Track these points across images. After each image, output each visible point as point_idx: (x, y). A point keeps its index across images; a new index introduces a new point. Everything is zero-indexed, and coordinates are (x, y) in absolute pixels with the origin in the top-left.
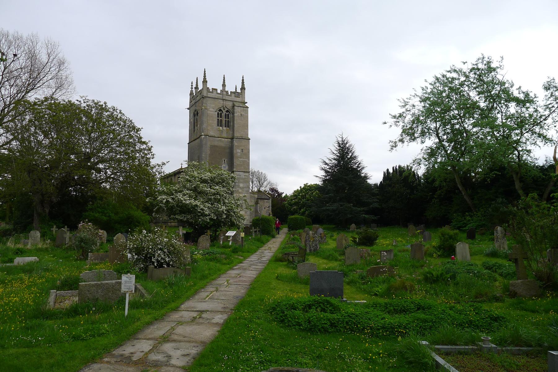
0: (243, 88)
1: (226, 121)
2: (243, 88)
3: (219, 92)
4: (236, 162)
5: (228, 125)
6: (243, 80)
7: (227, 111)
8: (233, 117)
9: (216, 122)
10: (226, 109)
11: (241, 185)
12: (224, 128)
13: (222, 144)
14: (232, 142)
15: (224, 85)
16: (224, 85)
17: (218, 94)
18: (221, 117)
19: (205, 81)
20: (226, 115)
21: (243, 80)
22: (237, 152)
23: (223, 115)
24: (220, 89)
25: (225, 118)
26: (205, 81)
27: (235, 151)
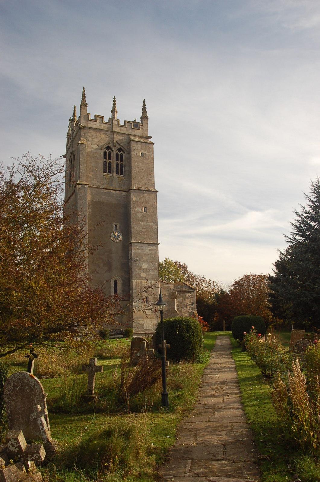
0: (144, 117)
1: (117, 165)
2: (144, 117)
3: (106, 120)
4: (135, 227)
7: (120, 150)
8: (130, 158)
9: (101, 165)
10: (118, 147)
11: (145, 266)
12: (115, 175)
14: (128, 197)
15: (113, 111)
16: (113, 111)
17: (105, 123)
18: (110, 158)
19: (84, 105)
20: (117, 156)
21: (144, 105)
22: (137, 211)
23: (114, 155)
24: (107, 116)
25: (117, 160)
26: (84, 105)
27: (132, 211)
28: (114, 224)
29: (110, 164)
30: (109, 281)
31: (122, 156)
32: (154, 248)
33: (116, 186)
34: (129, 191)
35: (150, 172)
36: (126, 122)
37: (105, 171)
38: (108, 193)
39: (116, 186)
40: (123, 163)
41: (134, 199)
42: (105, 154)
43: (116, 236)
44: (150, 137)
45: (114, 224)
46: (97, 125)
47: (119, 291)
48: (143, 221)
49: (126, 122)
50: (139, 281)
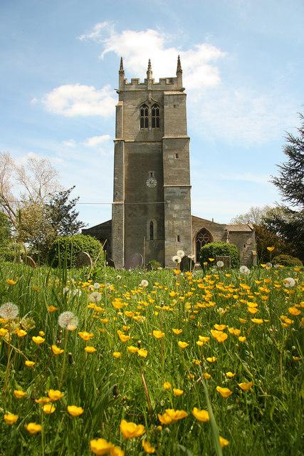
0: (179, 72)
1: (153, 119)
2: (179, 72)
3: (142, 81)
4: (167, 173)
5: (158, 126)
6: (179, 61)
8: (163, 112)
11: (177, 207)
13: (145, 151)
18: (147, 114)
20: (153, 111)
21: (179, 61)
22: (169, 157)
23: (150, 111)
27: (164, 158)
28: (150, 172)
29: (147, 120)
30: (146, 221)
31: (158, 111)
32: (186, 190)
33: (151, 138)
34: (161, 141)
35: (182, 121)
36: (160, 80)
37: (142, 126)
38: (144, 145)
39: (151, 138)
40: (159, 117)
41: (166, 147)
42: (142, 111)
43: (151, 183)
44: (184, 89)
45: (150, 172)
46: (133, 88)
47: (155, 232)
48: (175, 167)
49: (160, 80)
50: (171, 222)
